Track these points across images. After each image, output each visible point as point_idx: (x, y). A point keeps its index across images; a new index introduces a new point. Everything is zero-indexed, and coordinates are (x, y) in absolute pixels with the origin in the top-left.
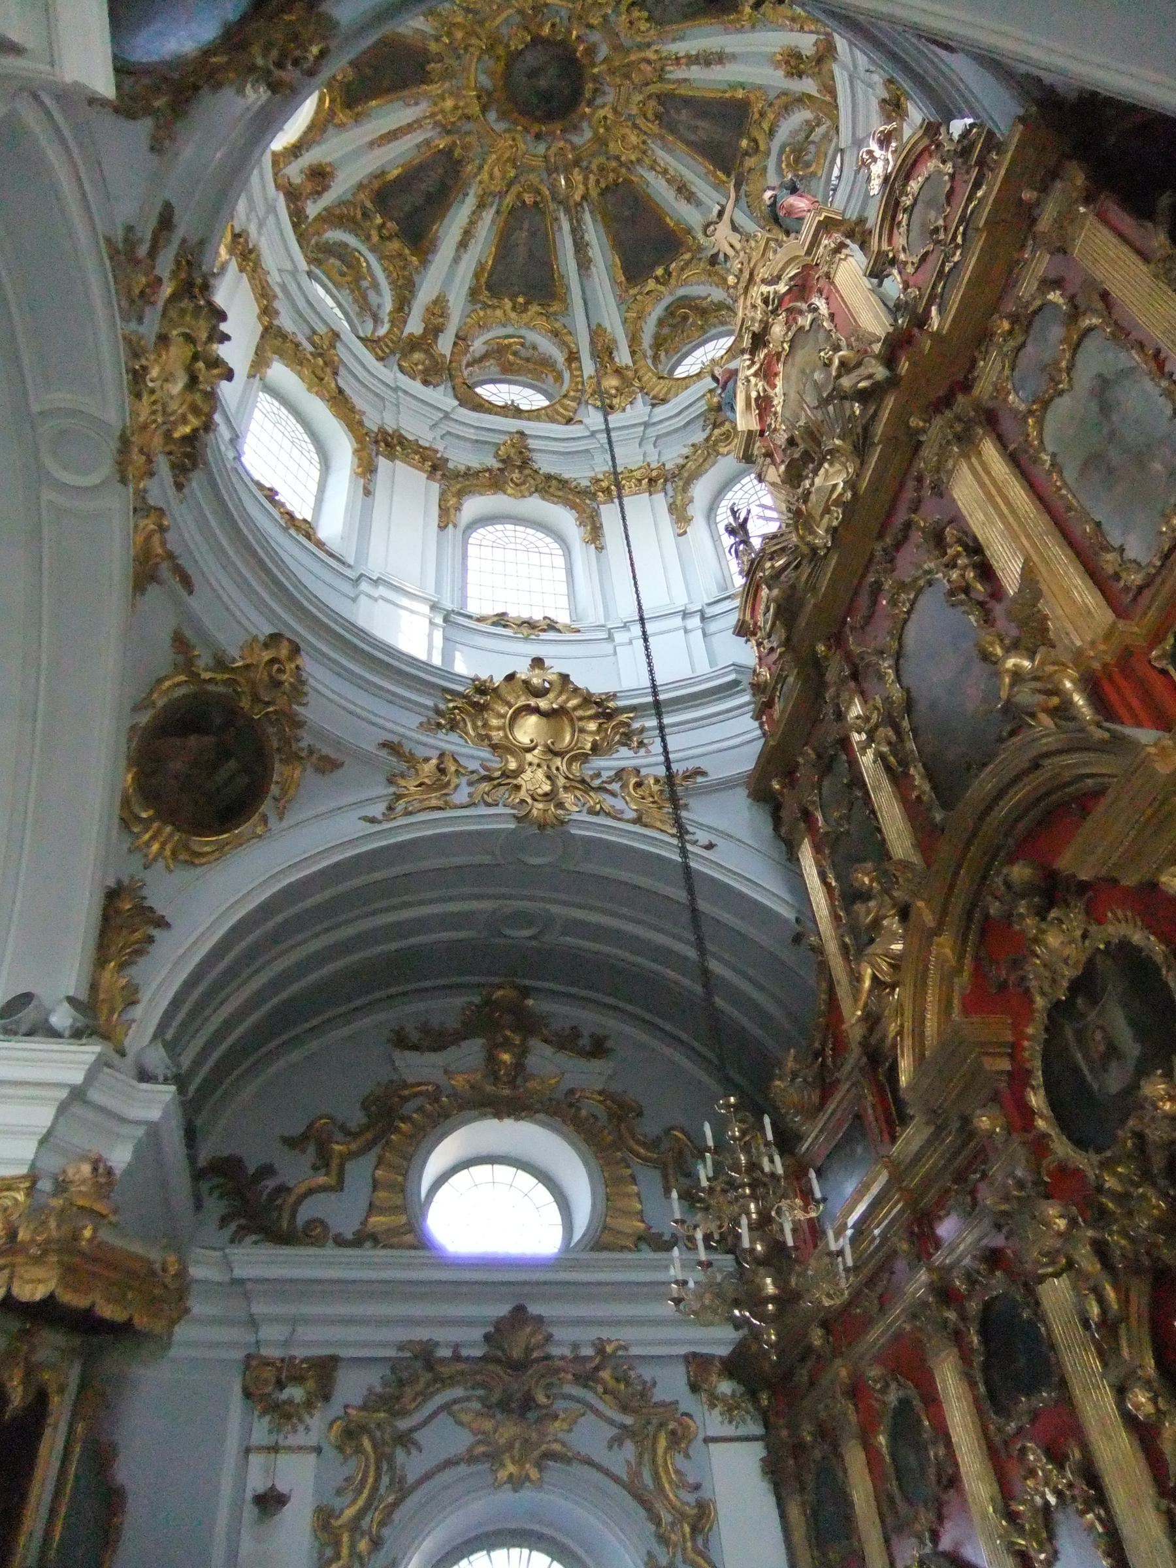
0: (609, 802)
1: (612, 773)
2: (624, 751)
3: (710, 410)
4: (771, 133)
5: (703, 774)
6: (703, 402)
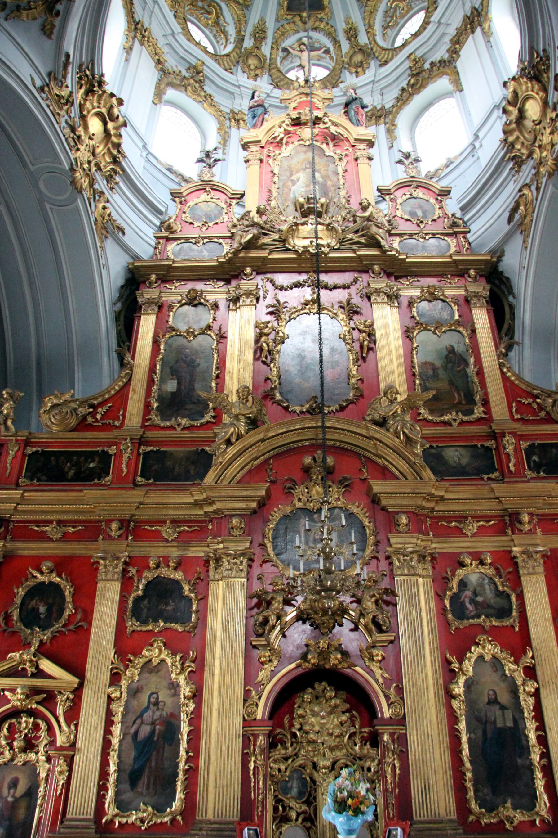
0: (92, 200)
1: (100, 190)
2: (105, 182)
3: (195, 67)
4: (315, 29)
5: (124, 233)
6: (196, 61)
